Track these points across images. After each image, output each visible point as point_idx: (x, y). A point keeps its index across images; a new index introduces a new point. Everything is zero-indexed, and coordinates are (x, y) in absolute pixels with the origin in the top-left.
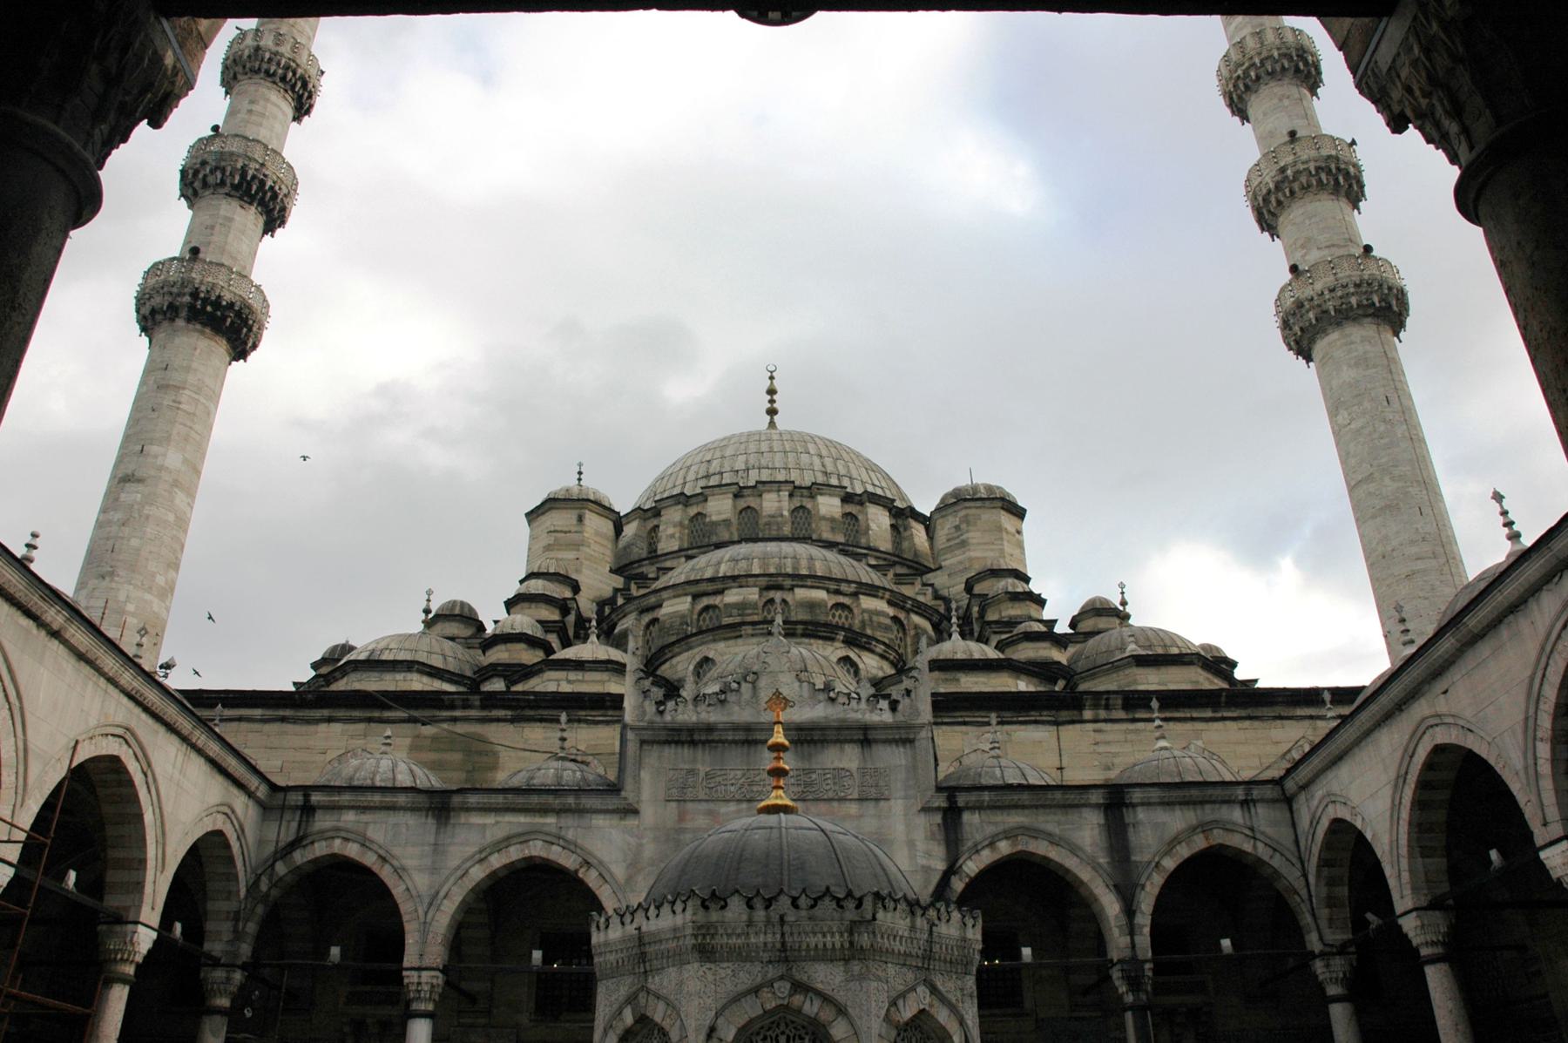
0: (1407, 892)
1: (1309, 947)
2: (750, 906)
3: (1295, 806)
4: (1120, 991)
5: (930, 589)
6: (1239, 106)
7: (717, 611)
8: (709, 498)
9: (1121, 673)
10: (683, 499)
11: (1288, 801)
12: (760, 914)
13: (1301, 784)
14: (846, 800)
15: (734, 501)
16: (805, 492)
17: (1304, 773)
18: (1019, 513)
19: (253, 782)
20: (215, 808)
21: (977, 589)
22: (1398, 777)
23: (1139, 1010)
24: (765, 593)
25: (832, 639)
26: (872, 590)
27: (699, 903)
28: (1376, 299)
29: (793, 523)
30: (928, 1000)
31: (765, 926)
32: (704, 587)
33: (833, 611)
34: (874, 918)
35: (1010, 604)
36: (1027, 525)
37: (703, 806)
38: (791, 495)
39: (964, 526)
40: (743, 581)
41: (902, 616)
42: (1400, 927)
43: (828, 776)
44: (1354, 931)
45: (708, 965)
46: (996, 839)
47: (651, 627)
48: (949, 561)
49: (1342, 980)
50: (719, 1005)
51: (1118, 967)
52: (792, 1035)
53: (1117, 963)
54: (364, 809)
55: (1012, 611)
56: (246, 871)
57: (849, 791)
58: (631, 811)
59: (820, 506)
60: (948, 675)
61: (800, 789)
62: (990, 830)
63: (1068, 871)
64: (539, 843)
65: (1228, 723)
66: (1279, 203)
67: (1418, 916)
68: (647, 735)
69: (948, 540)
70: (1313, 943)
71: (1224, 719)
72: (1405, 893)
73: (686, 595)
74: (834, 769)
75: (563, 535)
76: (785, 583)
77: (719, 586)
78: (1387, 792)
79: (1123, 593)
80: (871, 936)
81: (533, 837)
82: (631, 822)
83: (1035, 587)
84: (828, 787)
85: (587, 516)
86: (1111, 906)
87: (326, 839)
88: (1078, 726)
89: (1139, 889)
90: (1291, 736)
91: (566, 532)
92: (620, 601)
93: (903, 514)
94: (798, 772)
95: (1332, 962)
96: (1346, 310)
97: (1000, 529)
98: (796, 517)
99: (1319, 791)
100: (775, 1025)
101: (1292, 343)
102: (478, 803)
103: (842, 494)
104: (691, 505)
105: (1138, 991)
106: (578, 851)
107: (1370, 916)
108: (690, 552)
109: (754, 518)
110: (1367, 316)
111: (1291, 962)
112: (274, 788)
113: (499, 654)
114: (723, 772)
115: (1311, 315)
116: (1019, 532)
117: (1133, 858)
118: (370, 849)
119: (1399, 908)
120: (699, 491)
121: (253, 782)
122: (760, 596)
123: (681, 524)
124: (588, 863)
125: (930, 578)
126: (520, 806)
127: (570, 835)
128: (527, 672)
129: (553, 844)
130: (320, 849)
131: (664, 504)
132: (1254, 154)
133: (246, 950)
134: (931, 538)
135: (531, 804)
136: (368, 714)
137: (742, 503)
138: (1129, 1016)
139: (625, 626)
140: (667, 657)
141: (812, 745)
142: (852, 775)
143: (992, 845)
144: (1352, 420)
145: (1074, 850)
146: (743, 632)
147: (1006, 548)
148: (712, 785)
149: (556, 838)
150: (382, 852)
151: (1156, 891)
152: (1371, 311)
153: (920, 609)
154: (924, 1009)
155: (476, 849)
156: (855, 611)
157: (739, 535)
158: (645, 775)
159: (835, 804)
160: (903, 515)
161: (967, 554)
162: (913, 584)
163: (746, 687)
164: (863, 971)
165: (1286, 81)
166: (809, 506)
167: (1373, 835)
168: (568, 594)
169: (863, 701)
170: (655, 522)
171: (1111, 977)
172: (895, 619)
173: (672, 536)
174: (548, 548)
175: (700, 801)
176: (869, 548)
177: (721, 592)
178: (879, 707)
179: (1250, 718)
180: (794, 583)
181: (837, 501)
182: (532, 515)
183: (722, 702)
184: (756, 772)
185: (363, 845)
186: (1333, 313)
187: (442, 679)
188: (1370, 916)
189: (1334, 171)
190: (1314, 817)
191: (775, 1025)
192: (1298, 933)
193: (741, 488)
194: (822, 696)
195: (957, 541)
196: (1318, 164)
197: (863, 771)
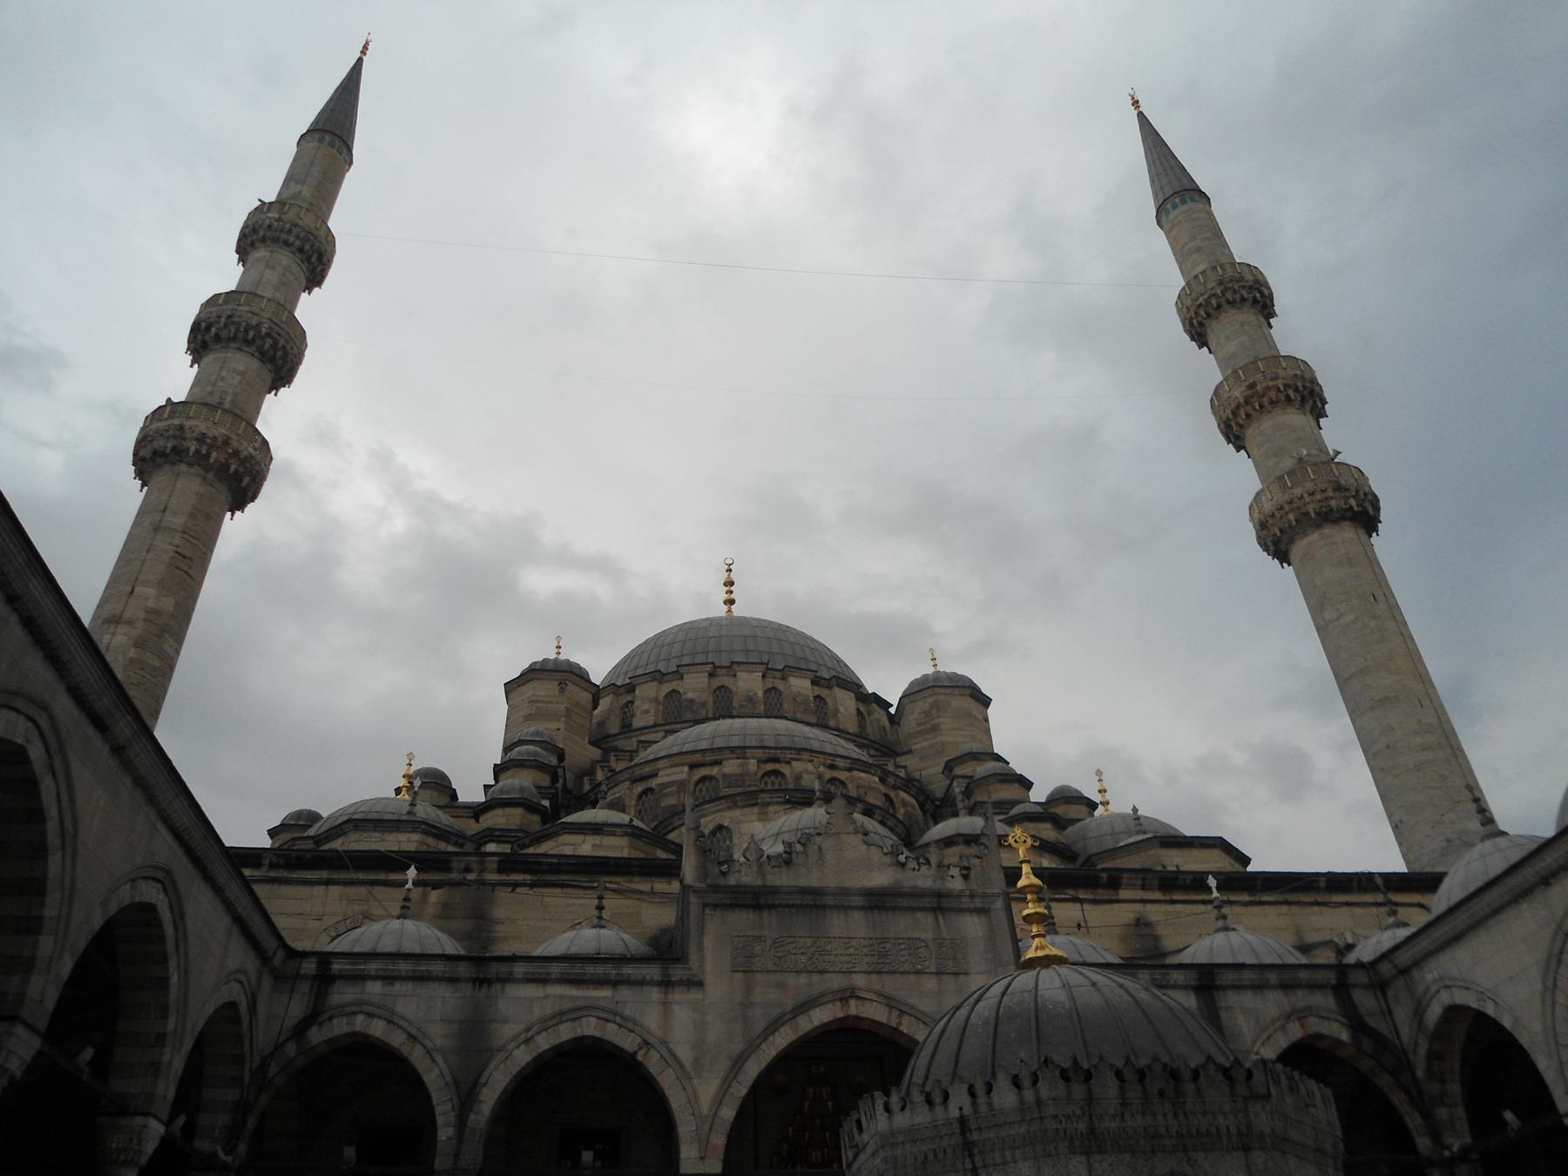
2: (1119, 1074)
5: (903, 770)
6: (1199, 330)
7: (714, 781)
8: (685, 676)
10: (658, 676)
14: (923, 973)
15: (709, 679)
16: (778, 675)
18: (985, 701)
21: (958, 771)
22: (1549, 959)
24: (762, 766)
26: (864, 767)
27: (1057, 1073)
28: (1353, 502)
29: (765, 704)
32: (697, 758)
35: (999, 786)
36: (992, 712)
37: (773, 977)
38: (764, 676)
39: (934, 711)
41: (892, 794)
43: (903, 946)
47: (644, 797)
48: (919, 745)
54: (389, 979)
58: (696, 984)
64: (593, 1020)
66: (1248, 416)
68: (711, 899)
69: (919, 725)
74: (908, 939)
75: (545, 705)
81: (585, 1013)
82: (694, 995)
84: (903, 959)
87: (347, 1015)
91: (547, 703)
92: (600, 775)
94: (871, 942)
96: (1326, 513)
98: (768, 698)
101: (1270, 544)
102: (525, 973)
103: (812, 677)
104: (665, 682)
106: (637, 1029)
108: (667, 728)
109: (728, 697)
110: (1344, 519)
112: (292, 954)
113: (497, 819)
114: (792, 940)
115: (1291, 517)
116: (987, 720)
118: (399, 1027)
120: (676, 669)
122: (758, 768)
123: (656, 700)
124: (648, 1044)
125: (902, 760)
126: (573, 977)
127: (627, 1012)
129: (608, 1021)
130: (339, 1027)
131: (639, 680)
132: (1216, 377)
135: (585, 974)
136: (372, 877)
137: (717, 682)
139: (617, 795)
140: (676, 825)
142: (927, 946)
144: (1340, 616)
146: (759, 801)
148: (779, 955)
149: (612, 1015)
150: (413, 1031)
152: (1349, 514)
155: (522, 1027)
157: (714, 714)
158: (708, 942)
159: (912, 978)
161: (939, 738)
163: (812, 849)
165: (1245, 309)
166: (780, 685)
168: (554, 761)
170: (629, 698)
172: (887, 796)
173: (647, 712)
174: (529, 718)
175: (768, 971)
177: (718, 763)
178: (950, 874)
180: (792, 756)
181: (807, 683)
182: (510, 687)
183: (788, 863)
184: (825, 940)
185: (390, 1022)
186: (1313, 515)
187: (447, 841)
189: (1301, 388)
193: (715, 667)
194: (887, 859)
195: (928, 726)
196: (1285, 381)
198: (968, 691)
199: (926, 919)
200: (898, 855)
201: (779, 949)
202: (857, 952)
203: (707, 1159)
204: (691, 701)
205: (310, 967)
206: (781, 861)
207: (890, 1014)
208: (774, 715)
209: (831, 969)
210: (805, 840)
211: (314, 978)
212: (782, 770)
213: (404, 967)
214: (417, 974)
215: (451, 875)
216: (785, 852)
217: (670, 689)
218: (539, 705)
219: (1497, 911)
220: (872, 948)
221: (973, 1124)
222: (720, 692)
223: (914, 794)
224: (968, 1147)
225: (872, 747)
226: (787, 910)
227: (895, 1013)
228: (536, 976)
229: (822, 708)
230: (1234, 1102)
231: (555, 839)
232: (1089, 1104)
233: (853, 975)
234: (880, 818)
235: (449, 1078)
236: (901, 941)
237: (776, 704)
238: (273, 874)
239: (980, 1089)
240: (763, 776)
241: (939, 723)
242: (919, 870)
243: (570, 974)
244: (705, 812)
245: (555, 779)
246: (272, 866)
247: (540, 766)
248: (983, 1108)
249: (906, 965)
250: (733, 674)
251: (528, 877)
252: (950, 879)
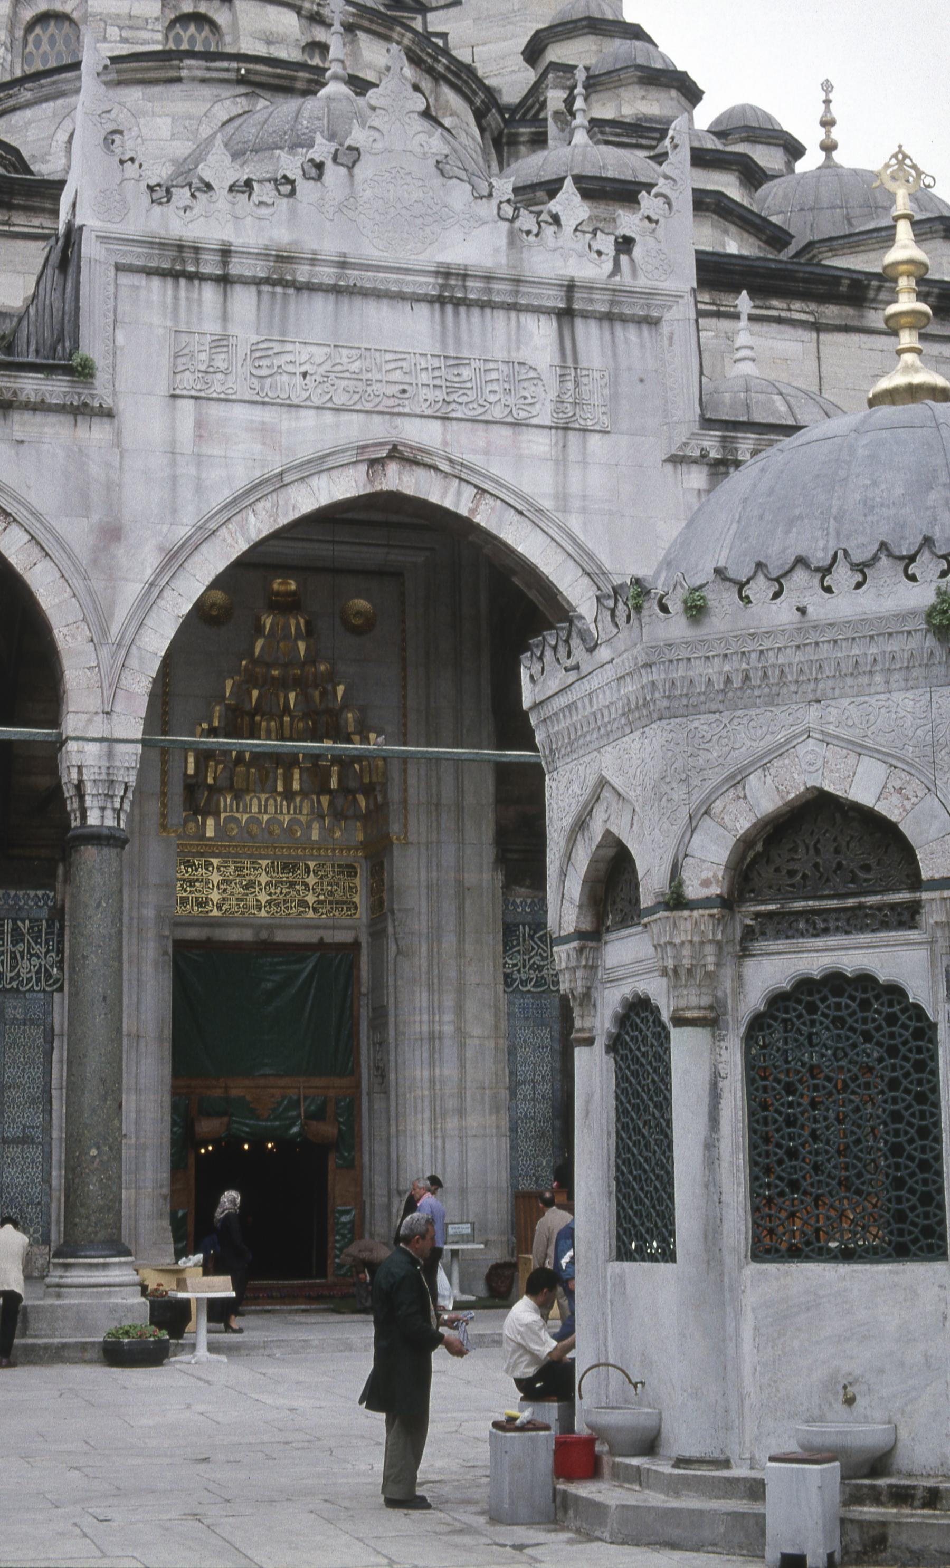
14: (527, 425)
21: (556, 53)
35: (639, 91)
43: (494, 375)
57: (535, 410)
61: (440, 395)
79: (827, 102)
84: (492, 398)
88: (855, 338)
146: (184, 73)
148: (264, 372)
178: (595, 247)
184: (353, 352)
201: (264, 362)
202: (407, 379)
203: (114, 716)
207: (459, 493)
209: (357, 407)
220: (437, 373)
226: (279, 290)
227: (469, 491)
233: (399, 421)
240: (173, 23)
242: (537, 235)
244: (64, 87)
252: (596, 256)
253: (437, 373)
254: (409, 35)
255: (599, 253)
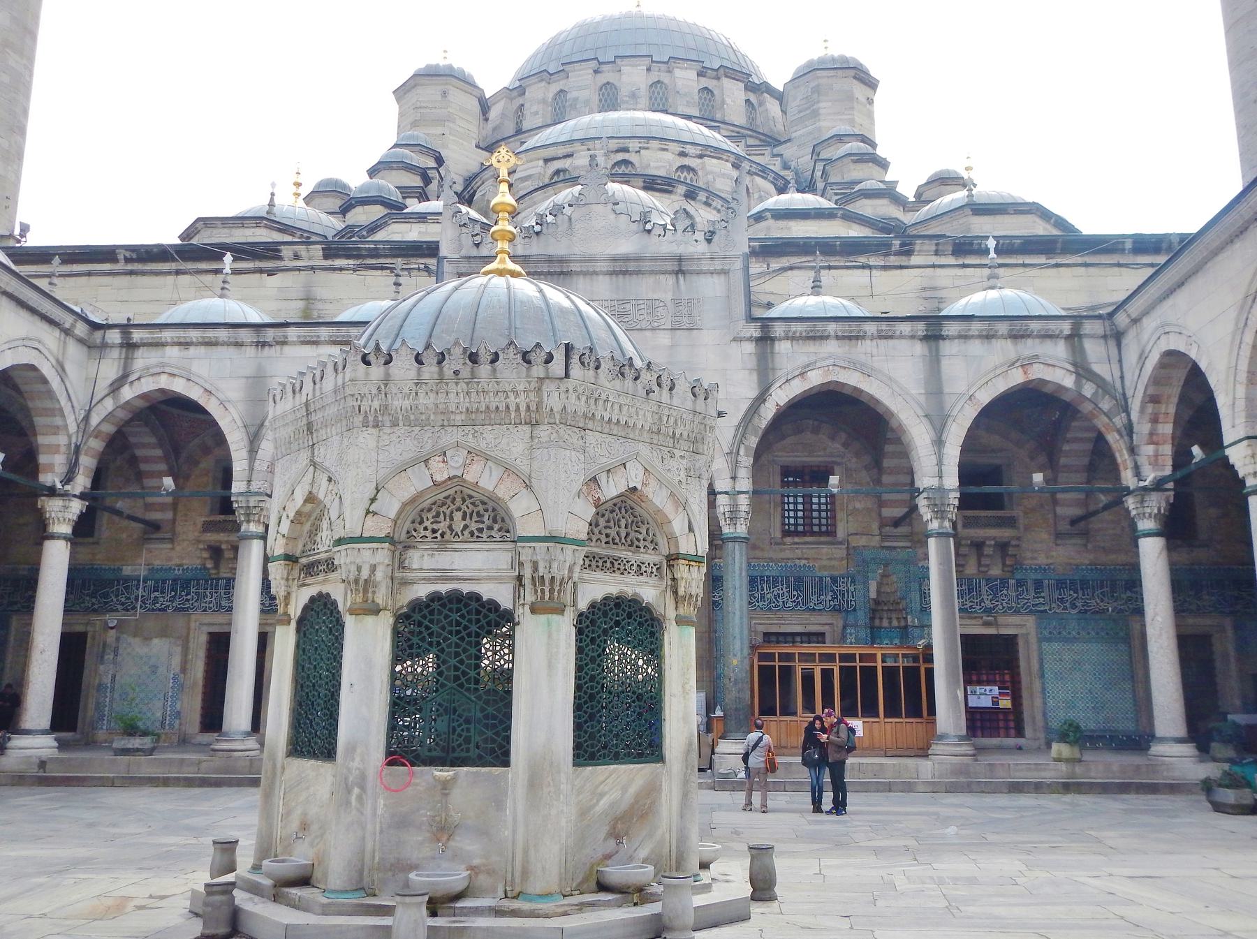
0: (1241, 419)
1: (1124, 483)
2: (418, 359)
3: (1124, 342)
4: (925, 519)
9: (955, 223)
11: (1118, 337)
12: (430, 370)
13: (1133, 316)
16: (664, 67)
17: (1134, 308)
18: (871, 84)
19: (68, 320)
20: (20, 343)
23: (940, 535)
24: (612, 156)
25: (670, 192)
27: (359, 357)
29: (651, 98)
30: (641, 476)
31: (437, 384)
33: (679, 173)
34: (567, 375)
35: (852, 166)
36: (879, 97)
38: (648, 70)
40: (590, 144)
42: (1227, 458)
43: (642, 306)
44: (1175, 467)
45: (370, 430)
46: (806, 370)
49: (1155, 515)
50: (382, 472)
51: (925, 495)
52: (468, 511)
53: (923, 491)
54: (186, 345)
55: (856, 172)
56: (73, 407)
57: (662, 321)
59: (677, 80)
60: (781, 223)
62: (802, 360)
63: (877, 401)
65: (1061, 269)
67: (1249, 446)
69: (799, 112)
70: (1128, 478)
71: (1057, 266)
72: (1237, 422)
73: (539, 159)
76: (630, 145)
77: (568, 149)
78: (1232, 314)
80: (563, 396)
83: (880, 152)
85: (450, 92)
86: (919, 435)
89: (950, 420)
90: (1125, 281)
93: (759, 90)
94: (613, 303)
95: (1147, 498)
97: (851, 98)
98: (653, 92)
99: (1150, 324)
100: (449, 501)
102: (299, 337)
103: (699, 68)
104: (555, 82)
105: (943, 518)
107: (1196, 450)
109: (613, 94)
111: (1103, 499)
112: (95, 326)
113: (362, 216)
116: (870, 101)
117: (946, 390)
119: (1228, 436)
121: (68, 320)
123: (544, 101)
128: (375, 227)
130: (148, 385)
133: (82, 482)
134: (784, 112)
137: (602, 79)
138: (932, 542)
139: (483, 192)
141: (627, 276)
143: (802, 374)
145: (889, 381)
147: (857, 119)
151: (968, 424)
153: (763, 172)
154: (635, 489)
156: (700, 173)
159: (648, 334)
160: (758, 88)
162: (764, 154)
164: (553, 437)
166: (665, 78)
167: (1209, 364)
168: (432, 164)
169: (680, 231)
170: (520, 101)
171: (917, 506)
173: (536, 113)
176: (724, 123)
177: (570, 156)
179: (1086, 265)
180: (641, 145)
181: (693, 75)
182: (401, 93)
187: (292, 234)
188: (1196, 450)
190: (1143, 352)
191: (449, 501)
192: (1114, 470)
193: (600, 63)
194: (635, 226)
195: (808, 112)
197: (677, 301)
198: (852, 73)
199: (670, 280)
200: (646, 223)
204: (576, 99)
205: (114, 337)
206: (532, 232)
208: (659, 109)
210: (557, 210)
211: (121, 346)
212: (631, 159)
213: (194, 334)
214: (206, 340)
215: (283, 263)
216: (537, 223)
217: (558, 90)
218: (422, 111)
219: (1216, 253)
220: (613, 308)
221: (312, 409)
222: (606, 89)
223: (771, 179)
224: (309, 426)
225: (750, 136)
228: (308, 339)
229: (710, 100)
230: (529, 382)
231: (386, 229)
232: (386, 385)
234: (704, 199)
235: (240, 423)
236: (641, 302)
237: (661, 99)
238: (130, 267)
239: (318, 378)
241: (819, 108)
243: (337, 336)
245: (427, 180)
246: (128, 260)
247: (409, 168)
248: (318, 393)
249: (644, 322)
250: (618, 69)
251: (351, 262)
253: (613, 308)
254: (732, 156)
255: (696, 241)
